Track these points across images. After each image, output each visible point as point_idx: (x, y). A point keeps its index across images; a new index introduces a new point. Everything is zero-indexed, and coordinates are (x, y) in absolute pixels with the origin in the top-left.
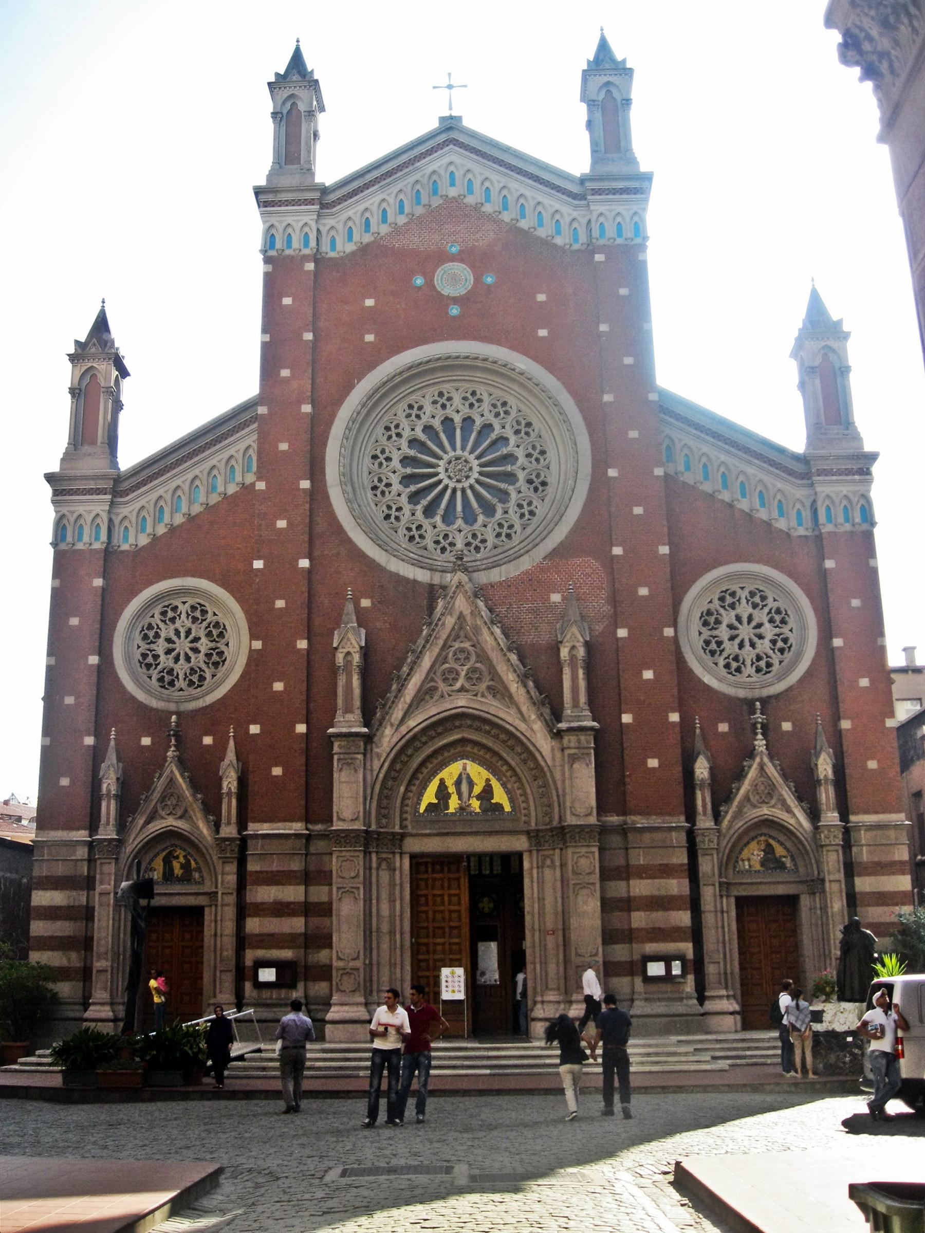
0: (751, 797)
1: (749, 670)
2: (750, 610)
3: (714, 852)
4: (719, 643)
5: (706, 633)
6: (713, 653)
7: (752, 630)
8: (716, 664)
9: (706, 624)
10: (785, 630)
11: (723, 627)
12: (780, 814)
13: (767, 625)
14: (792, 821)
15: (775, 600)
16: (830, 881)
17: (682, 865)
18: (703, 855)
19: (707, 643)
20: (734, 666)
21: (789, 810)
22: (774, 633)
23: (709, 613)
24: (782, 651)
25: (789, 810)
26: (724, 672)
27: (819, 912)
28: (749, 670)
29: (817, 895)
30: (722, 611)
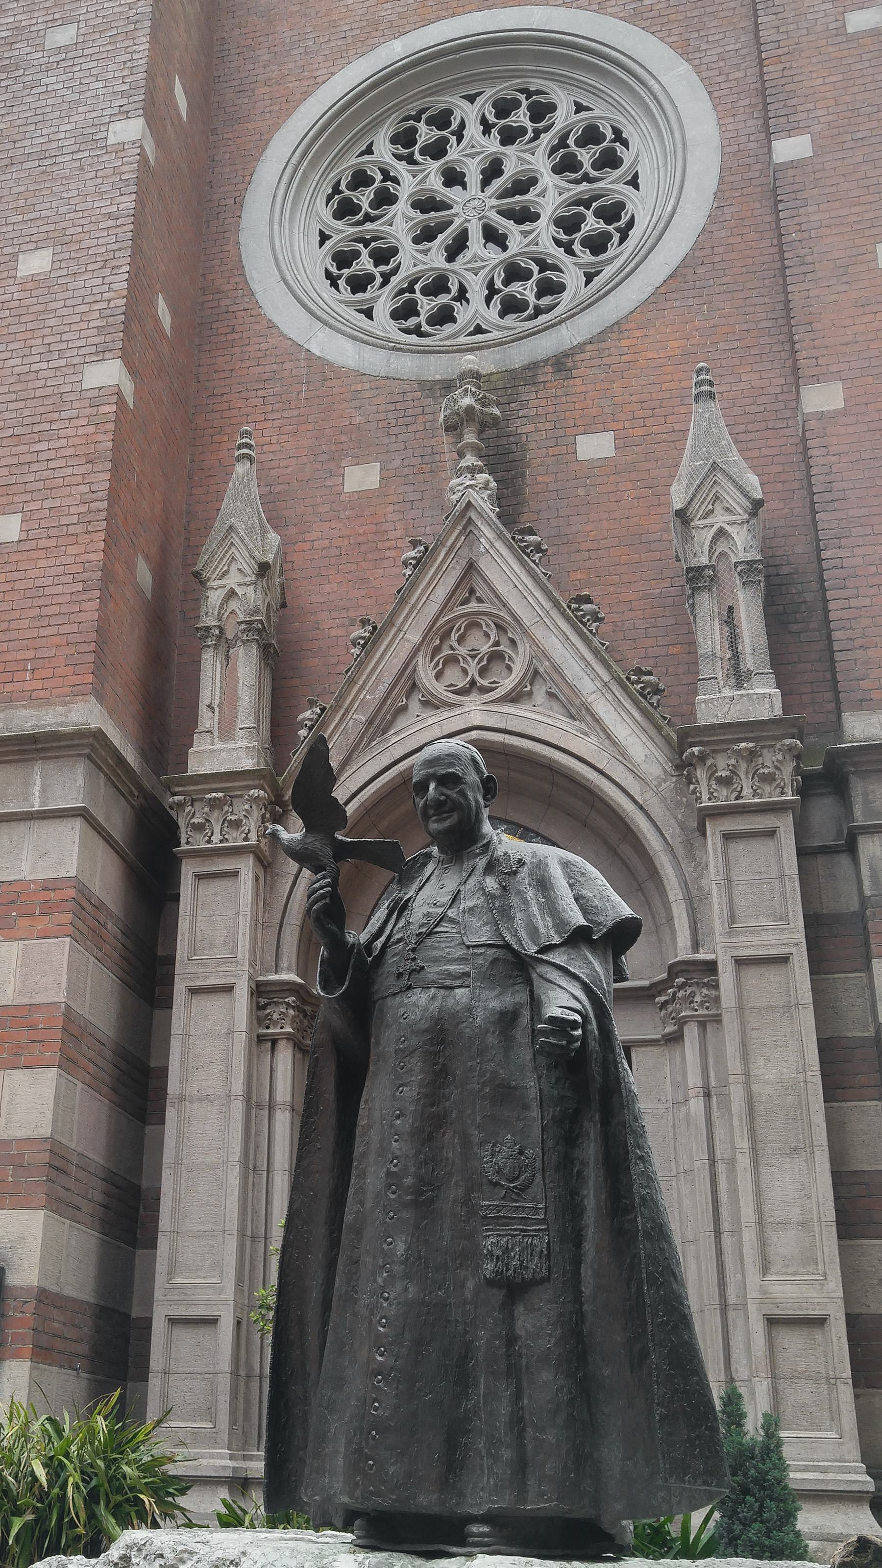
0: (425, 674)
1: (476, 309)
2: (492, 145)
3: (247, 867)
4: (382, 256)
5: (343, 231)
6: (359, 284)
7: (494, 202)
8: (368, 314)
9: (346, 210)
10: (611, 183)
11: (402, 208)
12: (539, 724)
13: (548, 180)
14: (587, 745)
15: (579, 108)
16: (740, 963)
17: (48, 886)
18: (199, 877)
19: (343, 259)
20: (426, 308)
21: (578, 711)
22: (565, 196)
23: (360, 180)
24: (597, 244)
25: (578, 711)
26: (391, 329)
27: (696, 1105)
28: (476, 309)
29: (691, 1032)
30: (401, 169)
